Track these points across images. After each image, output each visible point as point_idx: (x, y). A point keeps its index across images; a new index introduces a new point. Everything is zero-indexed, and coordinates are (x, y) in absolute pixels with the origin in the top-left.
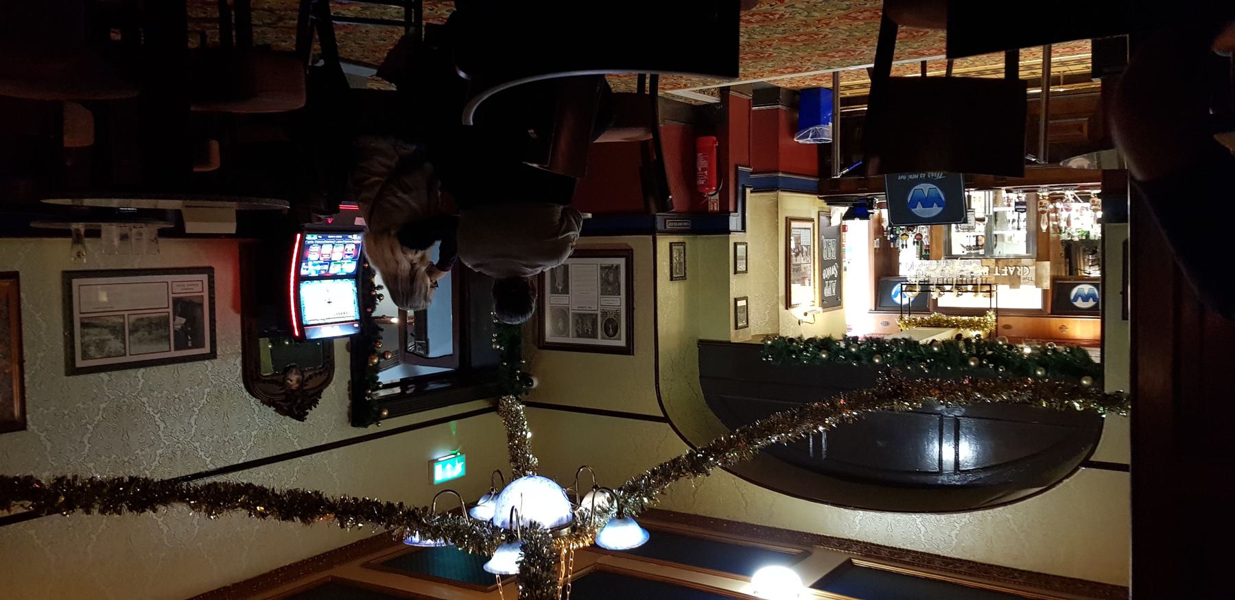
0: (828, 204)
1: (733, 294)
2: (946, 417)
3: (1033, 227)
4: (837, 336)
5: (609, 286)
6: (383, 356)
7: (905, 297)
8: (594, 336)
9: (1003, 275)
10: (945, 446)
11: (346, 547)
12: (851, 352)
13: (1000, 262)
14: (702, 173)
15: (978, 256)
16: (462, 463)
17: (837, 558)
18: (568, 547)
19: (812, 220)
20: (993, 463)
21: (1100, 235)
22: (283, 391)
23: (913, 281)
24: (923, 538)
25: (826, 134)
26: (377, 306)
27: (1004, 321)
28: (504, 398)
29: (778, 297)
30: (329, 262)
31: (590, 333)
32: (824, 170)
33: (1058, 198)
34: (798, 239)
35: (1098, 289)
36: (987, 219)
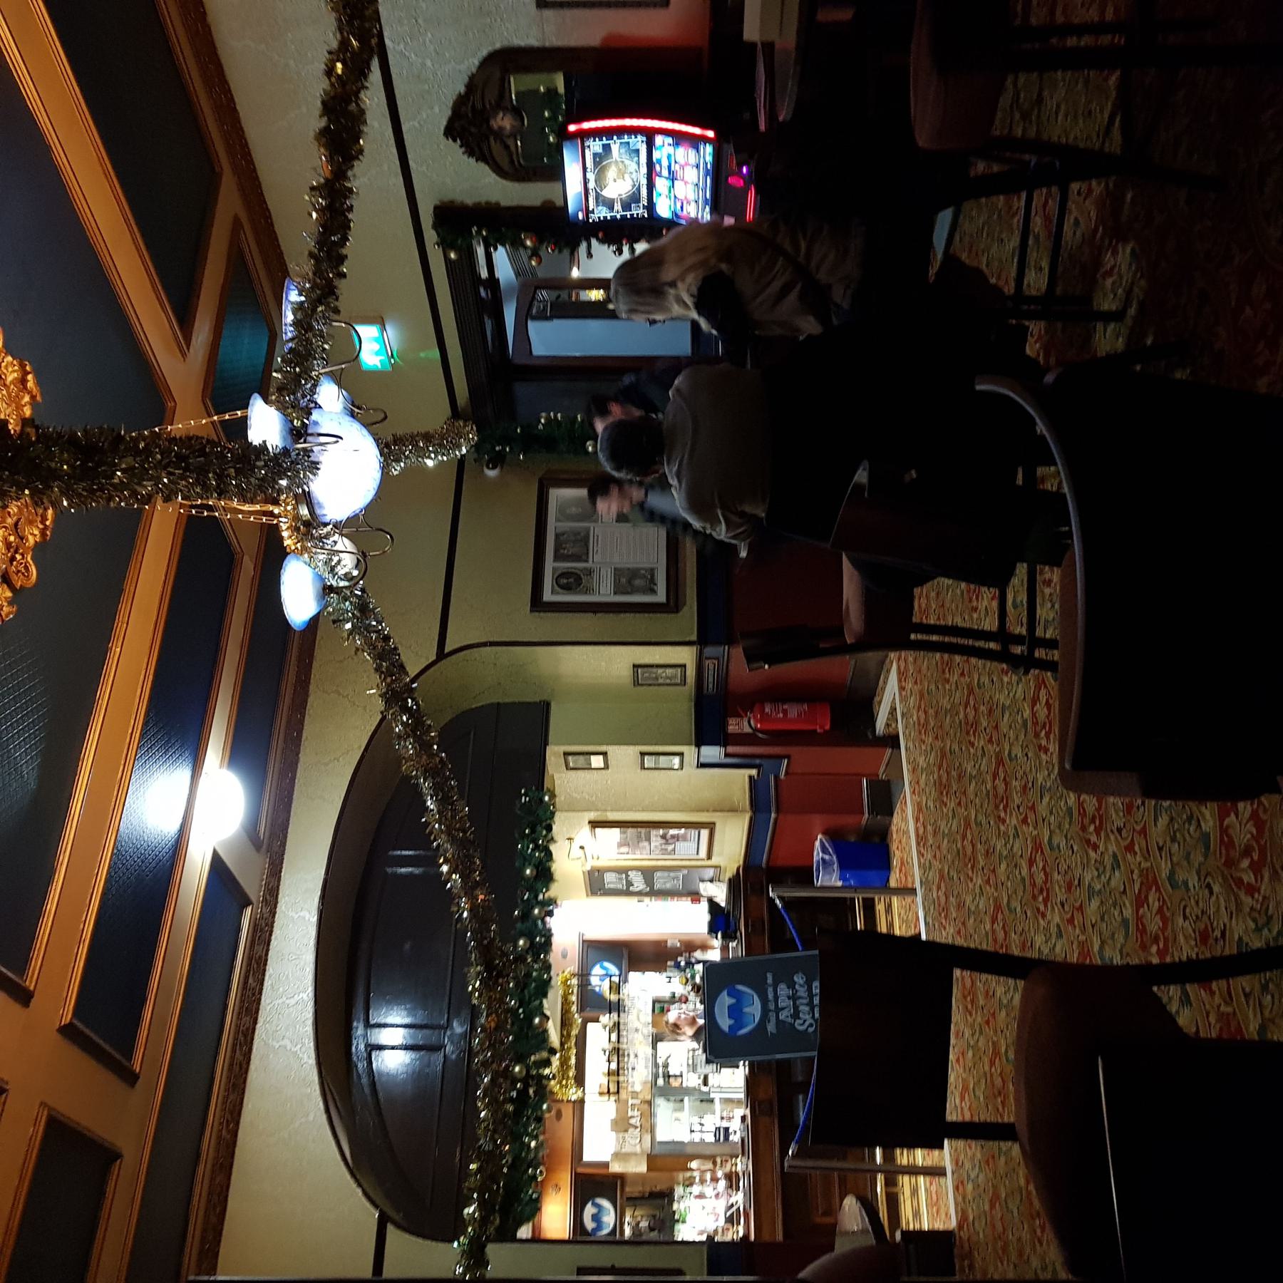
0: (730, 880)
1: (612, 750)
2: (444, 1034)
3: (689, 1150)
4: (554, 891)
5: (627, 579)
6: (535, 253)
7: (602, 980)
8: (557, 557)
9: (630, 1110)
10: (402, 1031)
11: (262, 194)
12: (533, 908)
13: (646, 1106)
14: (781, 709)
15: (656, 1077)
16: (380, 367)
17: (252, 886)
18: (284, 516)
19: (709, 857)
20: (381, 1095)
21: (680, 1239)
22: (488, 106)
23: (627, 990)
24: (280, 1001)
25: (827, 877)
26: (606, 245)
27: (567, 1112)
28: (475, 428)
29: (606, 810)
30: (672, 177)
31: (562, 551)
32: (777, 875)
33: (731, 1182)
34: (684, 838)
35: (609, 1234)
36: (705, 1089)
